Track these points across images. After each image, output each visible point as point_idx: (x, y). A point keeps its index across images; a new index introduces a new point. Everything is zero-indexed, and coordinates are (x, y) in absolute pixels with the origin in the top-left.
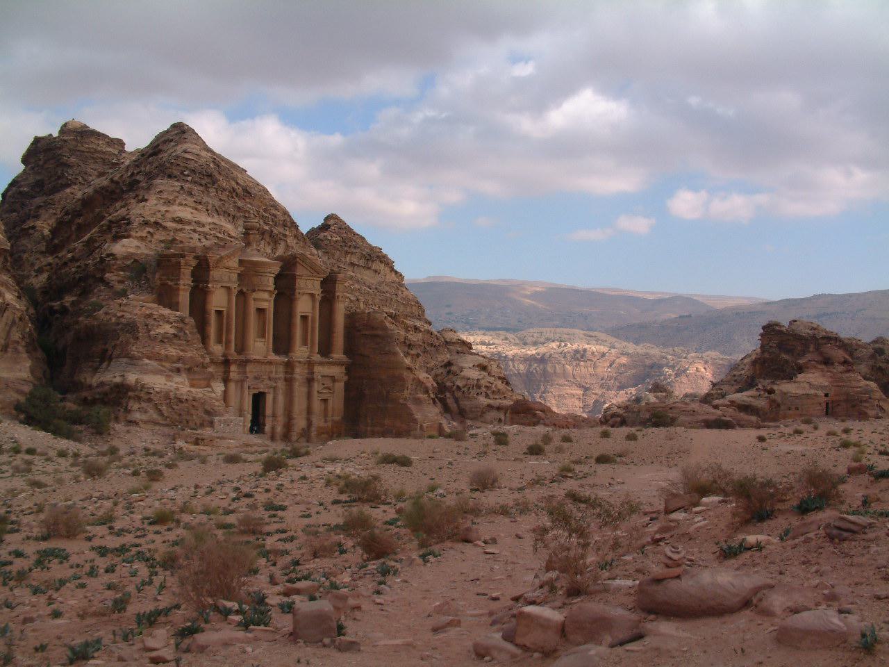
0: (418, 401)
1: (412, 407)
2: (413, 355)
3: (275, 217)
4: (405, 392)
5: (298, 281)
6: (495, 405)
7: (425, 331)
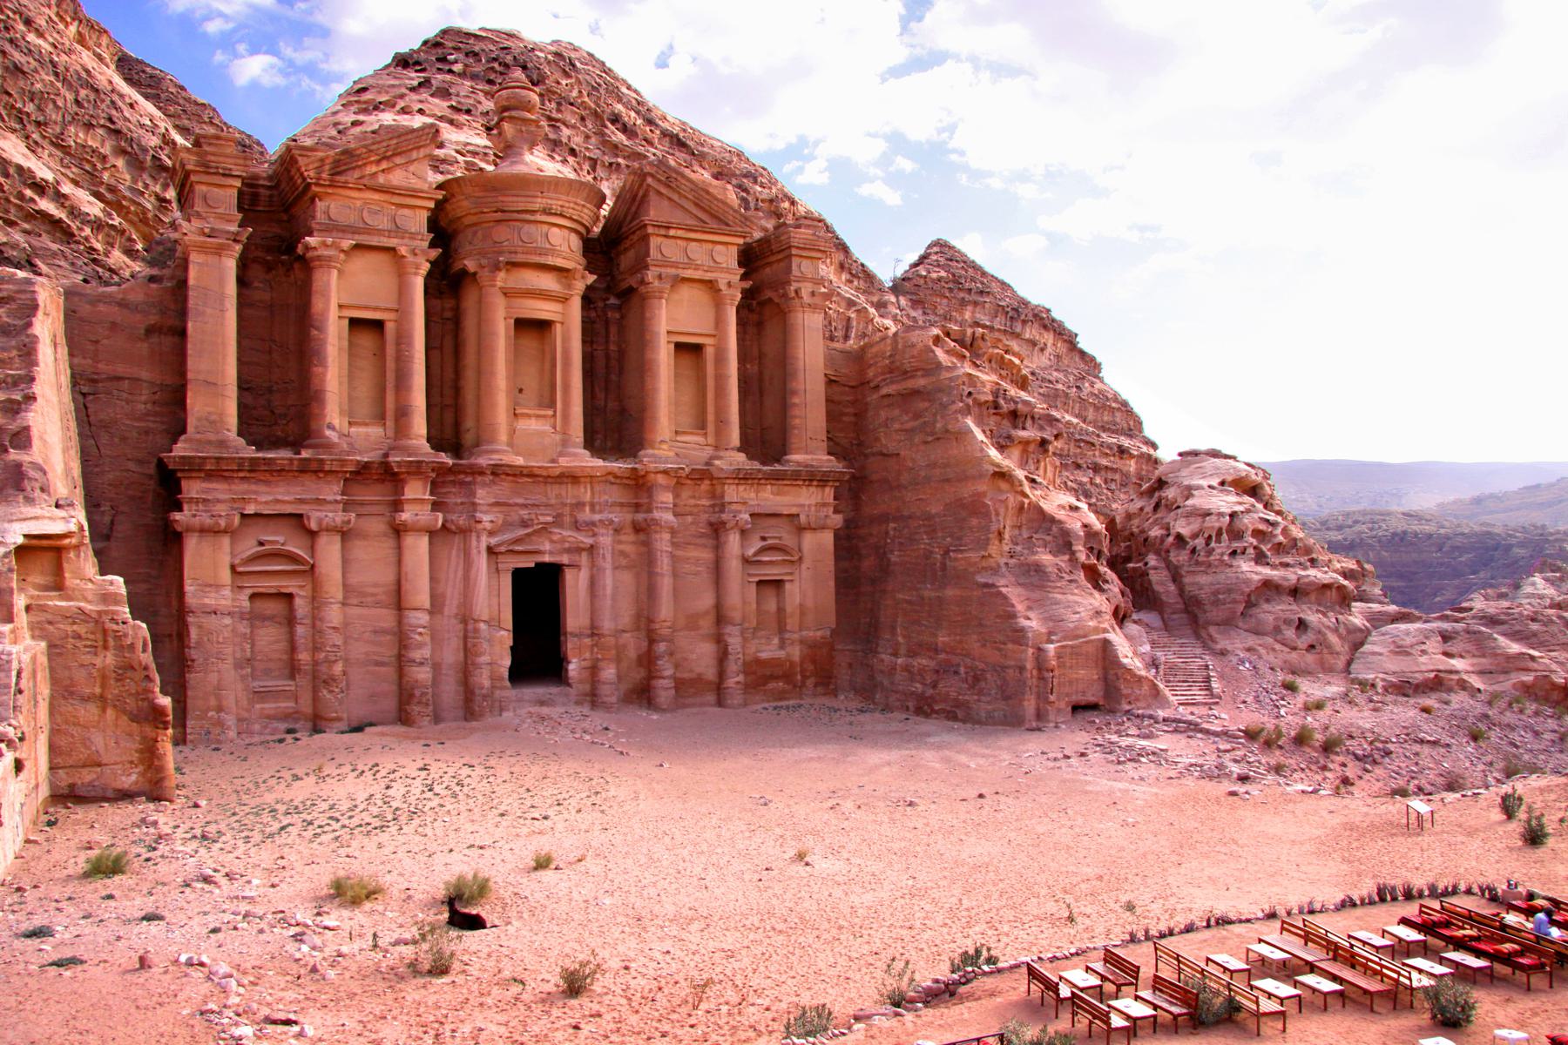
0: (1034, 576)
1: (1015, 595)
2: (1026, 443)
3: (746, 190)
4: (993, 549)
5: (654, 242)
6: (1286, 584)
7: (1142, 455)
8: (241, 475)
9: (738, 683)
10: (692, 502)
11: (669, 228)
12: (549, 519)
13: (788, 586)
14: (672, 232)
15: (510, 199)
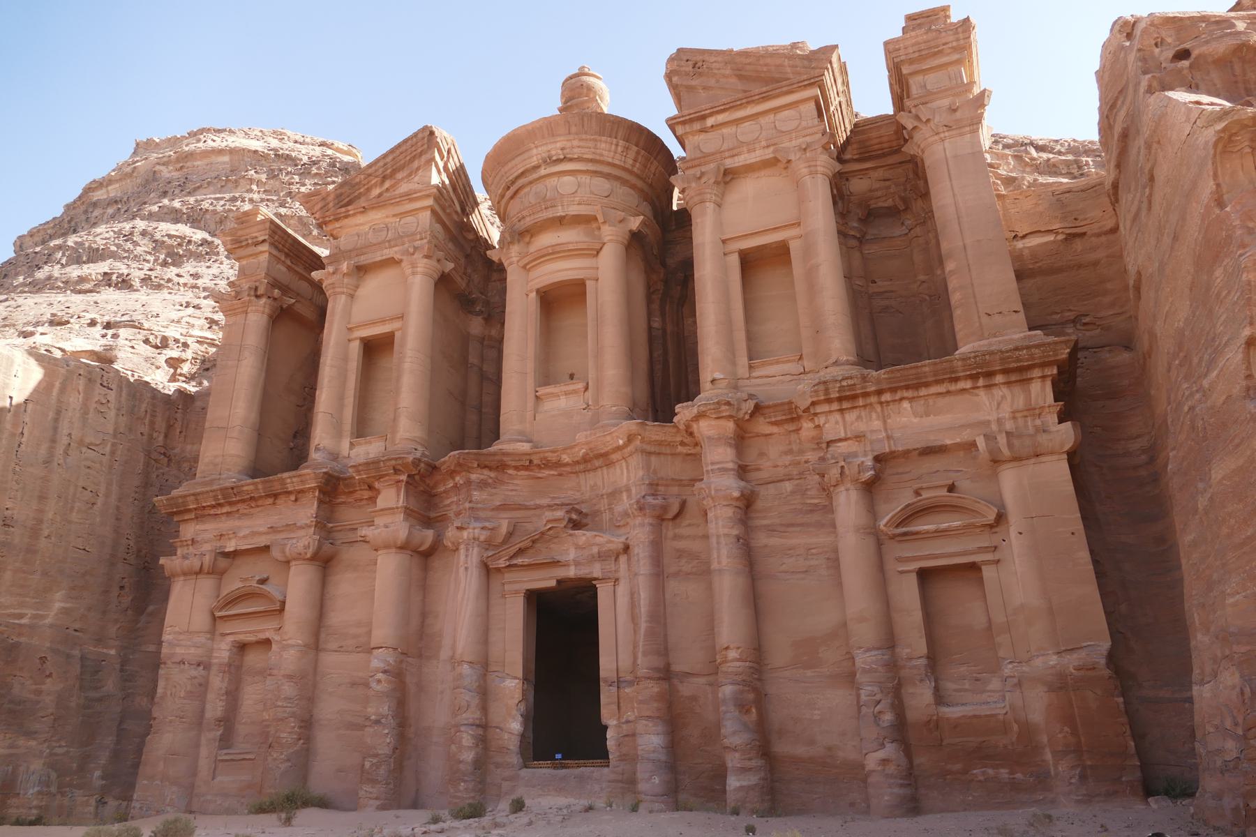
8: (225, 510)
9: (885, 762)
10: (788, 459)
11: (704, 118)
12: (559, 514)
13: (987, 572)
14: (710, 122)
15: (510, 165)
